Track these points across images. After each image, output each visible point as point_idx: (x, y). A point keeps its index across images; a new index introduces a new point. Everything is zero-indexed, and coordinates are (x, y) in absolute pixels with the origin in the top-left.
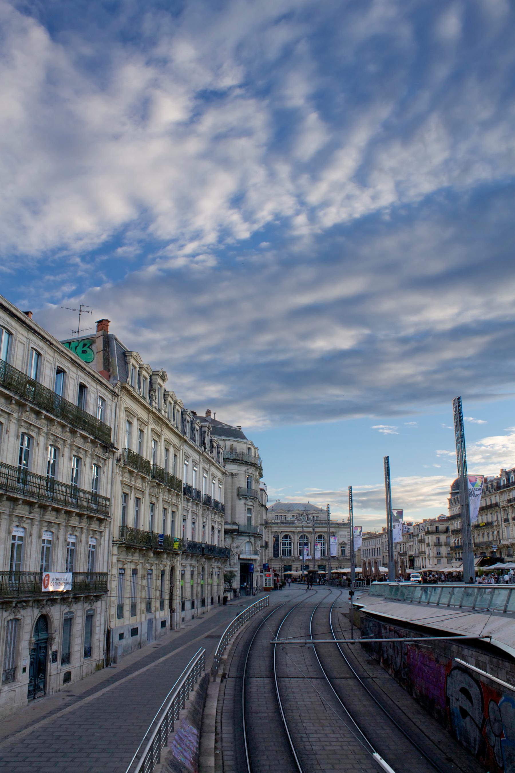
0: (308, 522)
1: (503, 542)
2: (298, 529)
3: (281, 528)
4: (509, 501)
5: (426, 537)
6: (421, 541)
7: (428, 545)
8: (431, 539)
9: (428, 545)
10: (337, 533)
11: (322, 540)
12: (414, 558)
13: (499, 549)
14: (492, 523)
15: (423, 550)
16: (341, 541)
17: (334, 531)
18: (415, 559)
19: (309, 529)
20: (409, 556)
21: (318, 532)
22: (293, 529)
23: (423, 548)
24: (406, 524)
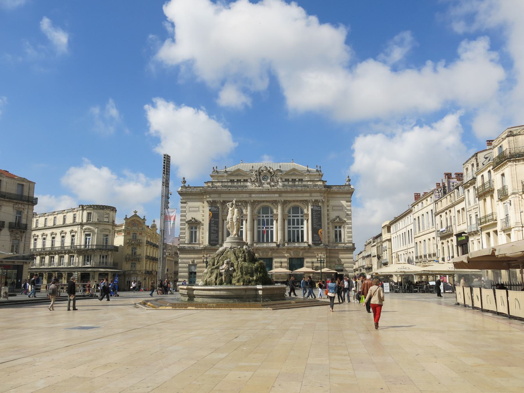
0: (272, 184)
2: (253, 195)
3: (222, 196)
5: (496, 177)
6: (484, 193)
7: (503, 195)
9: (503, 195)
10: (326, 204)
11: (300, 215)
12: (467, 238)
15: (489, 212)
16: (333, 215)
17: (318, 198)
18: (471, 239)
19: (273, 195)
20: (459, 235)
21: (290, 202)
22: (245, 195)
23: (493, 206)
24: (453, 176)
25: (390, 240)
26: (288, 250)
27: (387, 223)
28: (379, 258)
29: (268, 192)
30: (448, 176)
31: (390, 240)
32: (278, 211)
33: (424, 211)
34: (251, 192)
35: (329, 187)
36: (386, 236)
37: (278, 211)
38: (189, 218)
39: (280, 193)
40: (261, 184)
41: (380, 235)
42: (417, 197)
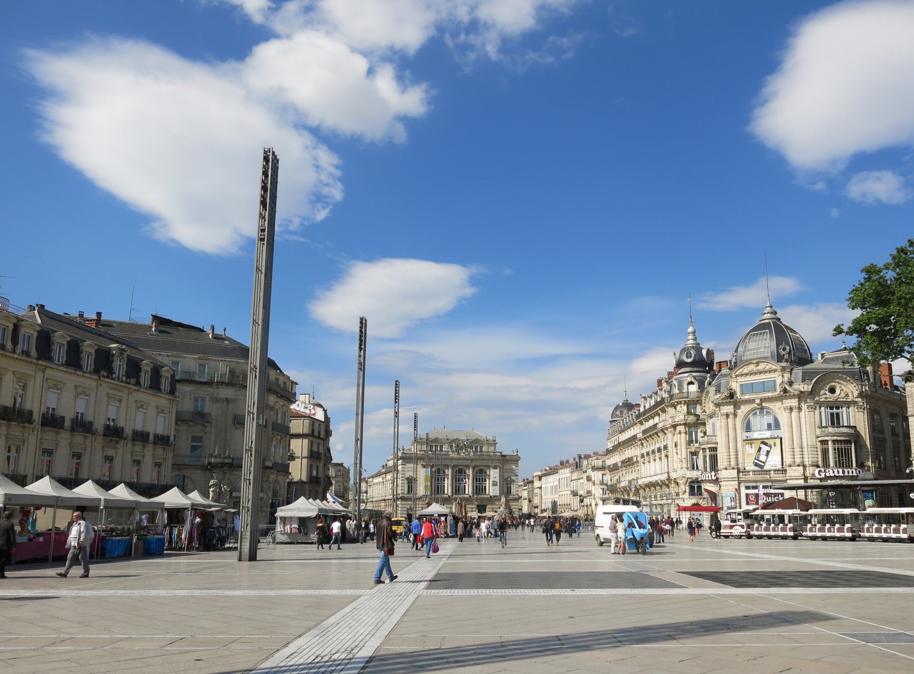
1: (640, 482)
4: (644, 432)
8: (597, 476)
13: (637, 490)
14: (632, 458)
25: (540, 488)
26: (477, 499)
27: (539, 473)
28: (530, 501)
29: (464, 459)
30: (580, 457)
31: (540, 488)
32: (470, 472)
33: (565, 476)
34: (452, 459)
35: (504, 456)
36: (537, 484)
37: (470, 472)
38: (407, 476)
39: (472, 460)
40: (459, 453)
41: (532, 482)
42: (562, 463)
